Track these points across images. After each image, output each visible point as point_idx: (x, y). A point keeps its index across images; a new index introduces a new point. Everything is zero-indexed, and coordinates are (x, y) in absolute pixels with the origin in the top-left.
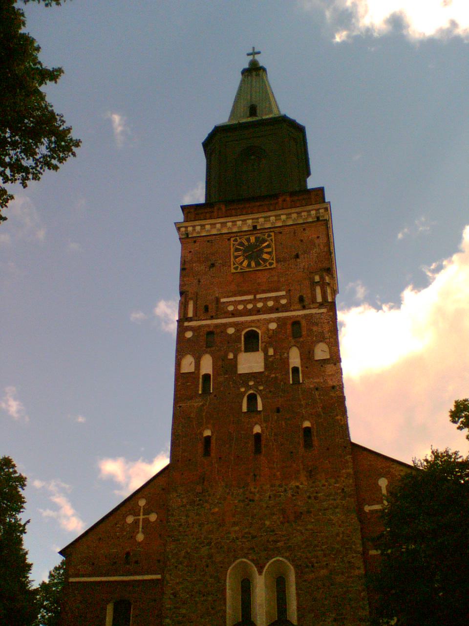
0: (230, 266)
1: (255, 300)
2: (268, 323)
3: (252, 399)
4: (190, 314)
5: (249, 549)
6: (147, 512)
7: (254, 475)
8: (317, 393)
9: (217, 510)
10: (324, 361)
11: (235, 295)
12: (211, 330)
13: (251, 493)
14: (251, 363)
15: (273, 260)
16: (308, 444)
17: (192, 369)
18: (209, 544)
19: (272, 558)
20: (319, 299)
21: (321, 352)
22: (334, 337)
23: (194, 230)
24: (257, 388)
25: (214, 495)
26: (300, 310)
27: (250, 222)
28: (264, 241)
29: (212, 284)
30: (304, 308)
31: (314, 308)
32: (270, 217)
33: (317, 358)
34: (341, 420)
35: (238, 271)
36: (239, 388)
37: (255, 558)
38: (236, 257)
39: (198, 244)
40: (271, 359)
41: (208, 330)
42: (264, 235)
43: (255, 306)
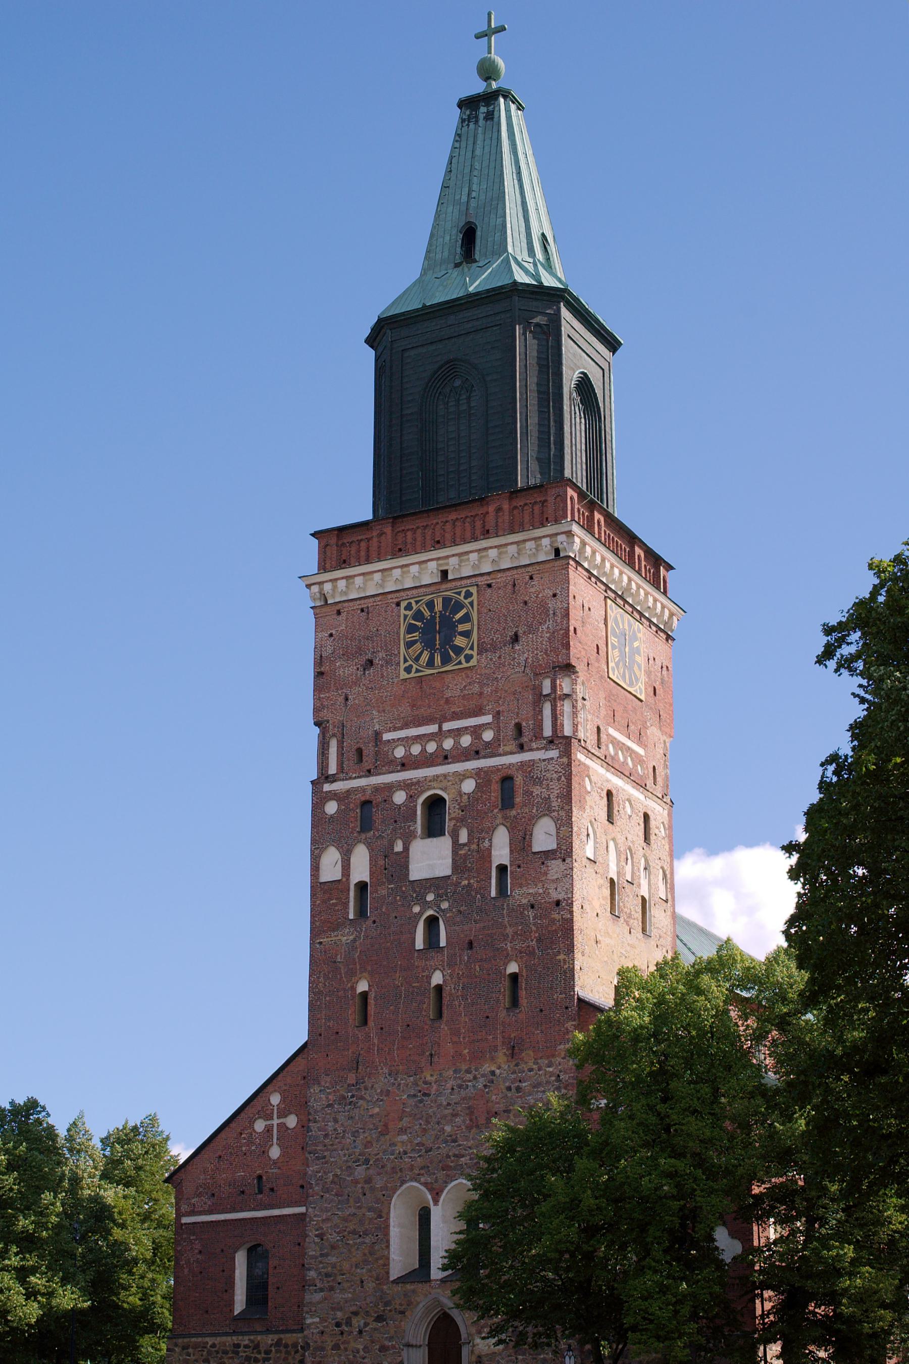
0: (399, 663)
1: (439, 736)
2: (461, 781)
3: (432, 923)
4: (333, 769)
5: (422, 1168)
6: (283, 1114)
7: (431, 1055)
8: (531, 913)
9: (377, 1110)
10: (548, 855)
11: (406, 726)
12: (368, 798)
13: (425, 1083)
14: (430, 858)
15: (472, 648)
16: (515, 1002)
17: (337, 876)
18: (367, 1161)
19: (452, 1181)
20: (548, 732)
21: (543, 837)
22: (567, 807)
23: (334, 588)
24: (439, 907)
25: (372, 1086)
26: (514, 753)
27: (433, 565)
28: (459, 606)
29: (368, 704)
30: (521, 748)
31: (538, 749)
32: (467, 553)
33: (536, 849)
34: (564, 960)
35: (412, 675)
36: (410, 908)
37: (429, 1180)
38: (409, 645)
39: (344, 615)
40: (462, 852)
41: (363, 799)
42: (459, 593)
43: (440, 746)
